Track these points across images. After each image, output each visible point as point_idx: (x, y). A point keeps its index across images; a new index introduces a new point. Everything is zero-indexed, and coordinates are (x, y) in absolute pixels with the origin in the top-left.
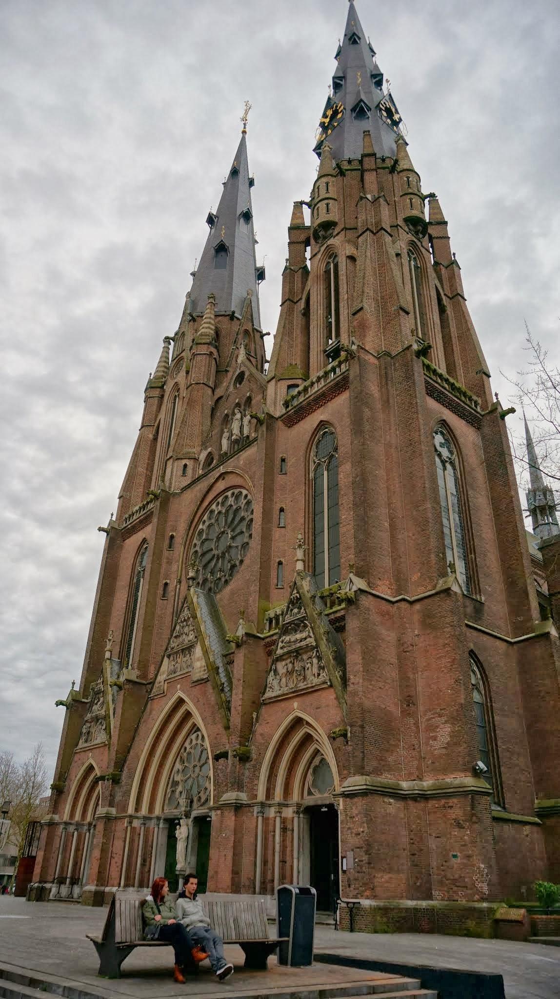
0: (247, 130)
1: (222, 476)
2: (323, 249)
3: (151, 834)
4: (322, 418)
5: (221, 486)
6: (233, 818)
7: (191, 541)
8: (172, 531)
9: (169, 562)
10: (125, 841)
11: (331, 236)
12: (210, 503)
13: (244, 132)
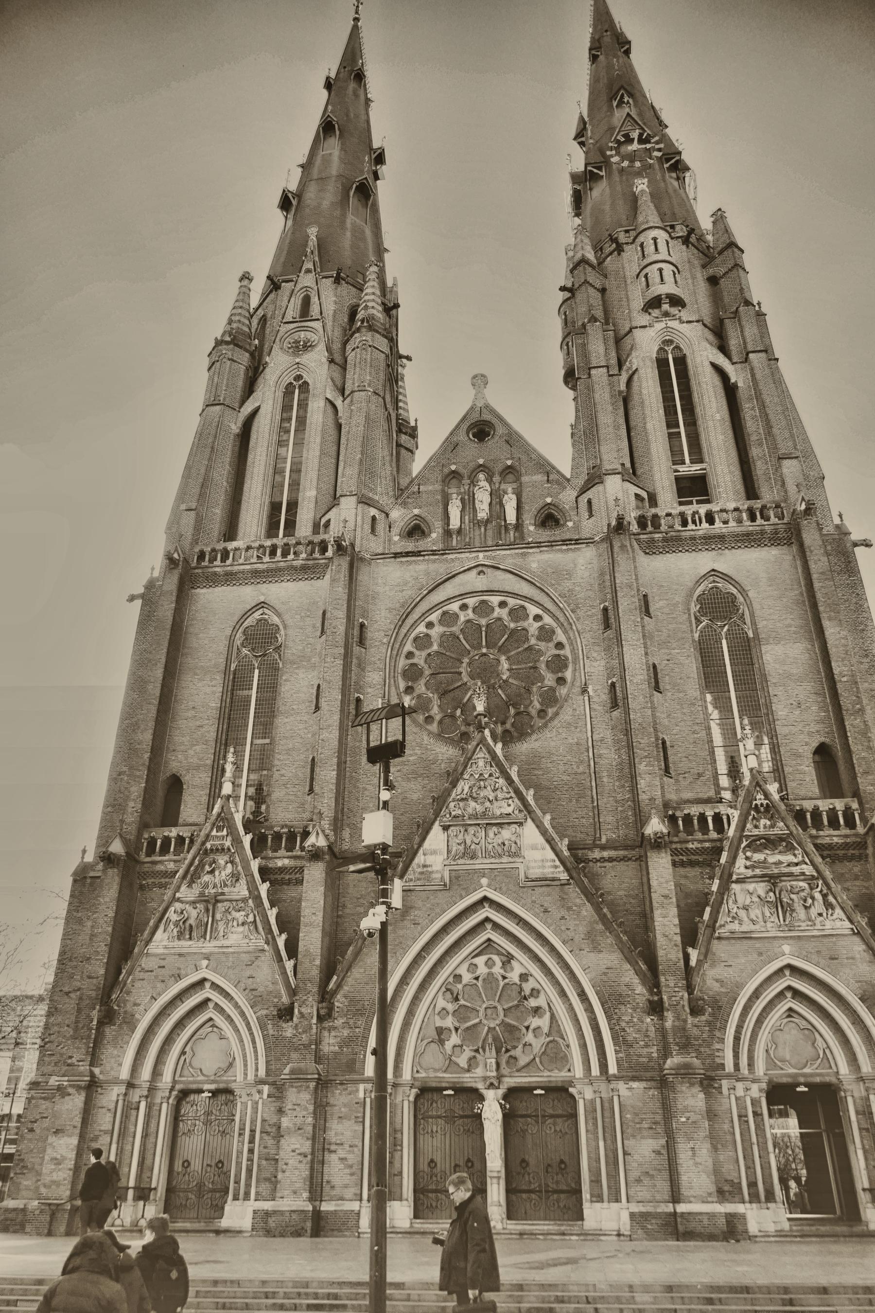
2: (659, 326)
3: (399, 1112)
6: (701, 1096)
7: (402, 645)
8: (363, 617)
9: (361, 666)
10: (363, 1122)
11: (673, 317)
13: (356, 20)
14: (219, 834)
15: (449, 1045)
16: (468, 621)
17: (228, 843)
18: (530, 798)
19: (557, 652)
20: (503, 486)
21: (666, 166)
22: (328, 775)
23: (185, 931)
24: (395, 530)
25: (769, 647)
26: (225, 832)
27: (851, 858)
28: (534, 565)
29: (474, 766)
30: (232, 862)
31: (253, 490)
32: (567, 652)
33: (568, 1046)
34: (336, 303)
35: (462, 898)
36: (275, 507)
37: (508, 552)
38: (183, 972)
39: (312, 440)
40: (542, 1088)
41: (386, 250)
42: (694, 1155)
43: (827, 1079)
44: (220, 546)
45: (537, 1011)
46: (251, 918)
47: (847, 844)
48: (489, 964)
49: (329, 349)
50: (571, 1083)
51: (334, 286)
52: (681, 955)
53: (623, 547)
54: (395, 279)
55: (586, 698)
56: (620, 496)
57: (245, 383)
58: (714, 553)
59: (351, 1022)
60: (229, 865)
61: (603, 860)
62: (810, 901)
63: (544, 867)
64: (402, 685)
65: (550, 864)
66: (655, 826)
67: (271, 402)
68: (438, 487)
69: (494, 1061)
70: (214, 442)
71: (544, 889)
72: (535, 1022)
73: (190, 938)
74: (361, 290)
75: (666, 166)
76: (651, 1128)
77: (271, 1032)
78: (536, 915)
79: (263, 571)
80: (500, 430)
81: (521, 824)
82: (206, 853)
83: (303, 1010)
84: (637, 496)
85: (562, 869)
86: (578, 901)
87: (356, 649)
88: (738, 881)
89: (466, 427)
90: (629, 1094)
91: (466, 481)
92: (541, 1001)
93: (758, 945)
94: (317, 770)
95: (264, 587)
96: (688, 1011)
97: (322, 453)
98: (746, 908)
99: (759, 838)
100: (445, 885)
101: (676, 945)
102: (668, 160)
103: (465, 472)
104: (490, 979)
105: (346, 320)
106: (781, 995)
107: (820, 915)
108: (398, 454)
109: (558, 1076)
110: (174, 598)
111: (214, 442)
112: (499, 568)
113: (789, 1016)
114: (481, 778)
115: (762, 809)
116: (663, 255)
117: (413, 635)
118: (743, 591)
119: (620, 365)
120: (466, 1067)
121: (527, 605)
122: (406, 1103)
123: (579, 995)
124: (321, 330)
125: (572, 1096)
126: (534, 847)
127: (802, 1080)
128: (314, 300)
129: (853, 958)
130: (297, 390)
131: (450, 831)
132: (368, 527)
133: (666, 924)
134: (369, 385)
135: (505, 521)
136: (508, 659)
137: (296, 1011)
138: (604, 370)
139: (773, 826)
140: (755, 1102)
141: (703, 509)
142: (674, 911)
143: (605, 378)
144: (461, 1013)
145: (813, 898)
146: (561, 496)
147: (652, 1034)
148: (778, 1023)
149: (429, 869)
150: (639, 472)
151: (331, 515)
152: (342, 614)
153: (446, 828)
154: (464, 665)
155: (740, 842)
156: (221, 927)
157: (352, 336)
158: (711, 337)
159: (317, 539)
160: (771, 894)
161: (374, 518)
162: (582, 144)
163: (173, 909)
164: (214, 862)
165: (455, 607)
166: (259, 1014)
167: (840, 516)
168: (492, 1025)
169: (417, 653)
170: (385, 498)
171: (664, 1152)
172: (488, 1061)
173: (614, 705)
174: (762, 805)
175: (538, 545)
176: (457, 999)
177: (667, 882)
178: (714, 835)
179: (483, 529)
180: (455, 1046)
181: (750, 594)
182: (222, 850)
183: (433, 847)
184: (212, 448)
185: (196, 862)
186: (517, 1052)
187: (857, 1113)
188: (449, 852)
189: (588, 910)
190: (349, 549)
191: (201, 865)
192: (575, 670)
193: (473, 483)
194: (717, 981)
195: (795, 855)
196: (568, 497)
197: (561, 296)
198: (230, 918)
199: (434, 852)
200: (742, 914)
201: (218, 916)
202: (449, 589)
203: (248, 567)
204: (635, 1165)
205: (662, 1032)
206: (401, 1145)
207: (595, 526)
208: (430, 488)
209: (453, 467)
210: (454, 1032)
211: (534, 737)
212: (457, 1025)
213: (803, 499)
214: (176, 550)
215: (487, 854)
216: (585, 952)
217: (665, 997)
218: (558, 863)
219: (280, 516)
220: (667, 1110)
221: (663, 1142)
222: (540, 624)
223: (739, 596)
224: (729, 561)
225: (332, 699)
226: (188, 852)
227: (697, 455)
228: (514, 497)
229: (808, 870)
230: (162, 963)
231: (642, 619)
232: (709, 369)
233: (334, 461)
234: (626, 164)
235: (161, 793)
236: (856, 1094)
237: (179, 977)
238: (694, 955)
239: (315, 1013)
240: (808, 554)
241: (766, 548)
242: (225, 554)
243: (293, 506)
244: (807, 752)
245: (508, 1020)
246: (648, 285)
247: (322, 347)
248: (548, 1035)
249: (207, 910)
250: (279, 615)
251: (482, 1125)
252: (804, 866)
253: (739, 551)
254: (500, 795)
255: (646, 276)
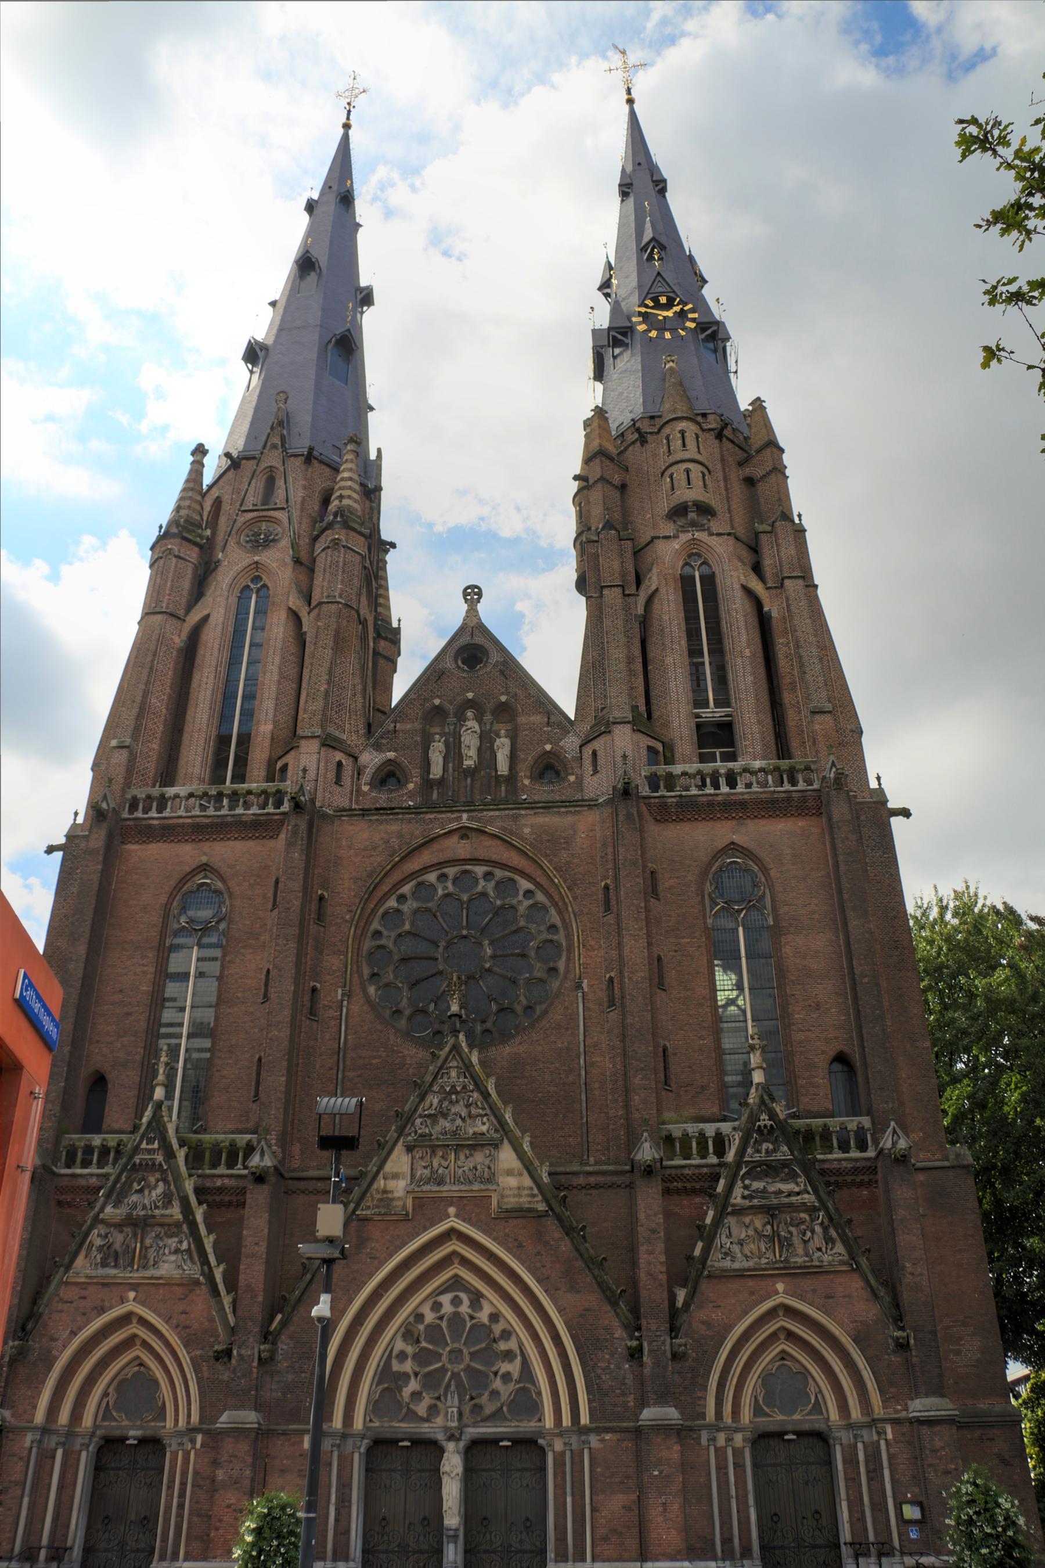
0: (352, 122)
1: (464, 833)
2: (684, 537)
4: (735, 838)
5: (461, 848)
6: (677, 1447)
7: (368, 922)
8: (323, 888)
11: (700, 527)
12: (426, 869)
14: (149, 1147)
15: (407, 1392)
16: (447, 895)
17: (159, 1158)
18: (508, 1117)
19: (550, 937)
20: (496, 727)
21: (702, 336)
22: (276, 1081)
23: (110, 1256)
24: (366, 778)
25: (790, 937)
26: (156, 1145)
27: (861, 1185)
28: (527, 830)
29: (445, 1076)
30: (165, 1181)
31: (198, 721)
32: (561, 937)
33: (539, 1394)
34: (305, 488)
35: (425, 1229)
36: (223, 741)
37: (497, 813)
38: (107, 1304)
39: (270, 659)
40: (509, 1440)
41: (372, 409)
42: (665, 1510)
43: (817, 1426)
44: (156, 791)
45: (508, 1356)
46: (185, 1246)
47: (856, 1169)
48: (456, 1302)
49: (294, 546)
50: (541, 1434)
51: (303, 467)
52: (665, 1296)
53: (629, 817)
54: (379, 451)
55: (580, 994)
56: (629, 753)
57: (192, 584)
58: (734, 822)
59: (297, 1365)
60: (161, 1184)
61: (588, 1187)
62: (809, 1234)
63: (520, 1196)
64: (366, 972)
65: (526, 1192)
66: (647, 1152)
67: (222, 610)
68: (417, 725)
69: (455, 1410)
70: (152, 661)
71: (518, 1221)
72: (505, 1367)
73: (115, 1266)
74: (337, 470)
75: (702, 336)
76: (622, 1483)
77: (206, 1375)
78: (509, 1250)
79: (207, 826)
80: (494, 657)
81: (496, 1146)
82: (135, 1168)
83: (243, 1352)
84: (650, 748)
85: (540, 1198)
86: (557, 1235)
87: (313, 928)
88: (734, 1213)
89: (454, 651)
90: (601, 1446)
91: (452, 719)
92: (512, 1345)
93: (751, 1283)
94: (263, 1074)
95: (206, 846)
96: (670, 1356)
97: (282, 676)
98: (741, 1243)
99: (760, 1164)
100: (407, 1215)
101: (661, 1285)
102: (704, 330)
103: (450, 708)
104: (456, 1319)
105: (316, 508)
106: (773, 1337)
107: (819, 1249)
108: (375, 664)
109: (526, 1427)
110: (101, 858)
111: (152, 661)
112: (485, 832)
113: (783, 1359)
114: (454, 1091)
115: (765, 1131)
116: (691, 452)
117: (381, 911)
118: (764, 869)
119: (639, 582)
120: (425, 1416)
121: (516, 877)
122: (356, 1456)
123: (552, 1339)
124: (285, 521)
125: (542, 1450)
126: (510, 1173)
127: (790, 1428)
128: (280, 483)
129: (849, 1296)
130: (255, 581)
131: (414, 1153)
132: (331, 775)
133: (652, 1260)
134: (340, 596)
135: (496, 771)
136: (491, 943)
137: (235, 1352)
138: (619, 590)
139: (775, 1150)
140: (738, 1453)
141: (722, 767)
142: (660, 1246)
143: (619, 599)
144: (423, 1357)
145: (813, 1231)
146: (562, 743)
147: (630, 1380)
148: (770, 1367)
149: (390, 1196)
150: (656, 715)
151: (289, 758)
152: (297, 885)
153: (409, 1149)
154: (441, 949)
155: (738, 1167)
156: (152, 1254)
157: (322, 532)
158: (744, 553)
159: (271, 787)
160: (769, 1227)
161: (340, 764)
162: (607, 295)
163: (96, 1231)
164: (144, 1179)
165: (432, 877)
166: (193, 1354)
167: (878, 778)
168: (456, 1370)
169: (385, 933)
170: (354, 737)
171: (635, 1507)
172: (450, 1410)
173: (611, 1003)
174: (765, 1126)
175: (532, 806)
176: (418, 1341)
177: (655, 1215)
178: (713, 1159)
179: (469, 780)
180: (413, 1394)
181: (772, 873)
182: (152, 1167)
183: (395, 1170)
184: (151, 668)
185: (123, 1179)
186: (484, 1399)
187: (845, 1462)
188: (413, 1176)
189: (565, 1246)
190: (309, 805)
191: (129, 1183)
192: (568, 960)
193: (461, 718)
194: (703, 1323)
195: (797, 1184)
196: (570, 743)
197: (575, 486)
198: (161, 1244)
199: (396, 1176)
200: (736, 1249)
201: (148, 1242)
202: (427, 857)
203: (189, 821)
204: (603, 1521)
205: (641, 1380)
206: (350, 1501)
207: (598, 785)
208: (409, 726)
209: (437, 702)
210: (413, 1378)
211: (518, 1040)
212: (417, 1369)
213: (833, 764)
214: (105, 798)
215: (457, 1180)
216: (561, 1292)
217: (645, 1344)
218: (536, 1191)
219: (228, 753)
220: (641, 1463)
221: (634, 1497)
222: (531, 902)
223: (760, 875)
224: (749, 833)
225: (284, 988)
226: (114, 1164)
227: (723, 701)
228: (506, 741)
229: (809, 1198)
230: (84, 1293)
231: (647, 902)
232: (739, 594)
233: (294, 686)
234: (653, 334)
235: (81, 1091)
236: (844, 1441)
237: (102, 1310)
238: (681, 1295)
239: (256, 1356)
240: (836, 830)
241: (793, 819)
242: (162, 802)
243: (245, 740)
244: (822, 1061)
245: (474, 1365)
246: (673, 488)
247: (285, 543)
248: (517, 1382)
249: (135, 1235)
250: (223, 880)
251: (440, 1479)
252: (806, 1196)
253: (763, 822)
254: (474, 1111)
255: (671, 476)
